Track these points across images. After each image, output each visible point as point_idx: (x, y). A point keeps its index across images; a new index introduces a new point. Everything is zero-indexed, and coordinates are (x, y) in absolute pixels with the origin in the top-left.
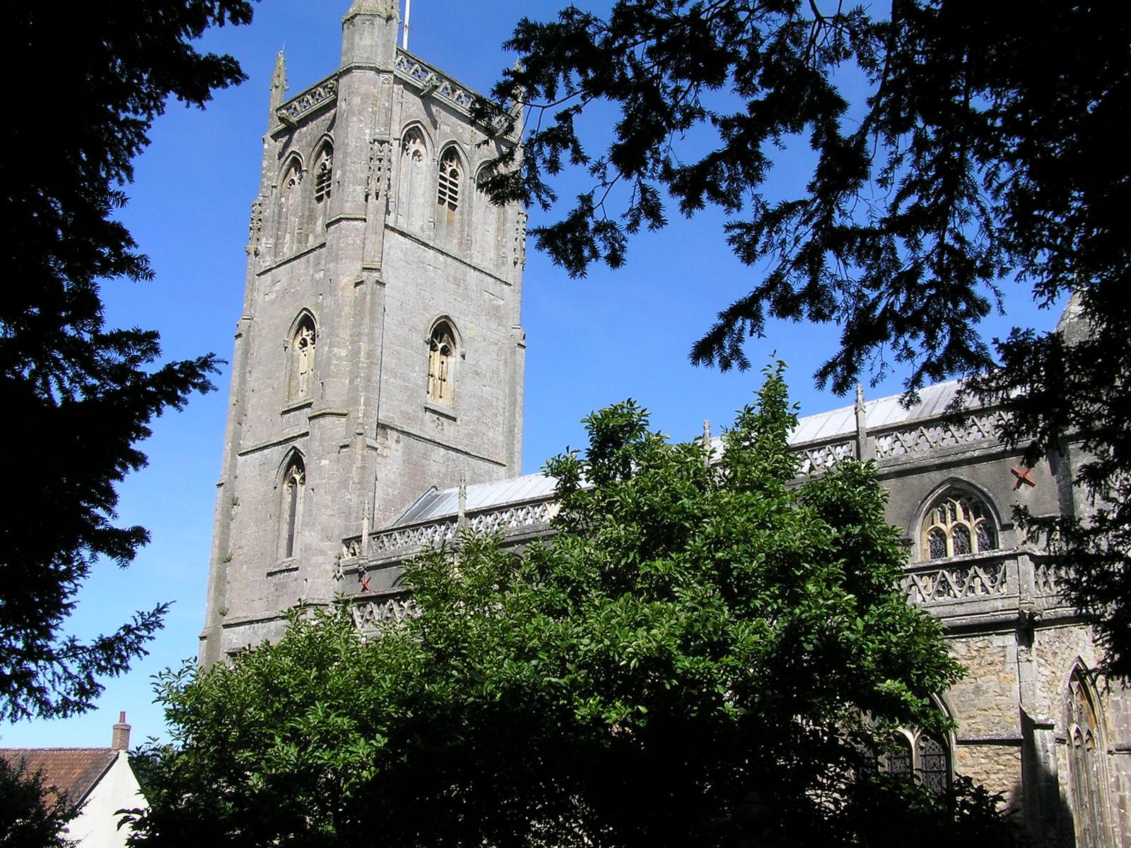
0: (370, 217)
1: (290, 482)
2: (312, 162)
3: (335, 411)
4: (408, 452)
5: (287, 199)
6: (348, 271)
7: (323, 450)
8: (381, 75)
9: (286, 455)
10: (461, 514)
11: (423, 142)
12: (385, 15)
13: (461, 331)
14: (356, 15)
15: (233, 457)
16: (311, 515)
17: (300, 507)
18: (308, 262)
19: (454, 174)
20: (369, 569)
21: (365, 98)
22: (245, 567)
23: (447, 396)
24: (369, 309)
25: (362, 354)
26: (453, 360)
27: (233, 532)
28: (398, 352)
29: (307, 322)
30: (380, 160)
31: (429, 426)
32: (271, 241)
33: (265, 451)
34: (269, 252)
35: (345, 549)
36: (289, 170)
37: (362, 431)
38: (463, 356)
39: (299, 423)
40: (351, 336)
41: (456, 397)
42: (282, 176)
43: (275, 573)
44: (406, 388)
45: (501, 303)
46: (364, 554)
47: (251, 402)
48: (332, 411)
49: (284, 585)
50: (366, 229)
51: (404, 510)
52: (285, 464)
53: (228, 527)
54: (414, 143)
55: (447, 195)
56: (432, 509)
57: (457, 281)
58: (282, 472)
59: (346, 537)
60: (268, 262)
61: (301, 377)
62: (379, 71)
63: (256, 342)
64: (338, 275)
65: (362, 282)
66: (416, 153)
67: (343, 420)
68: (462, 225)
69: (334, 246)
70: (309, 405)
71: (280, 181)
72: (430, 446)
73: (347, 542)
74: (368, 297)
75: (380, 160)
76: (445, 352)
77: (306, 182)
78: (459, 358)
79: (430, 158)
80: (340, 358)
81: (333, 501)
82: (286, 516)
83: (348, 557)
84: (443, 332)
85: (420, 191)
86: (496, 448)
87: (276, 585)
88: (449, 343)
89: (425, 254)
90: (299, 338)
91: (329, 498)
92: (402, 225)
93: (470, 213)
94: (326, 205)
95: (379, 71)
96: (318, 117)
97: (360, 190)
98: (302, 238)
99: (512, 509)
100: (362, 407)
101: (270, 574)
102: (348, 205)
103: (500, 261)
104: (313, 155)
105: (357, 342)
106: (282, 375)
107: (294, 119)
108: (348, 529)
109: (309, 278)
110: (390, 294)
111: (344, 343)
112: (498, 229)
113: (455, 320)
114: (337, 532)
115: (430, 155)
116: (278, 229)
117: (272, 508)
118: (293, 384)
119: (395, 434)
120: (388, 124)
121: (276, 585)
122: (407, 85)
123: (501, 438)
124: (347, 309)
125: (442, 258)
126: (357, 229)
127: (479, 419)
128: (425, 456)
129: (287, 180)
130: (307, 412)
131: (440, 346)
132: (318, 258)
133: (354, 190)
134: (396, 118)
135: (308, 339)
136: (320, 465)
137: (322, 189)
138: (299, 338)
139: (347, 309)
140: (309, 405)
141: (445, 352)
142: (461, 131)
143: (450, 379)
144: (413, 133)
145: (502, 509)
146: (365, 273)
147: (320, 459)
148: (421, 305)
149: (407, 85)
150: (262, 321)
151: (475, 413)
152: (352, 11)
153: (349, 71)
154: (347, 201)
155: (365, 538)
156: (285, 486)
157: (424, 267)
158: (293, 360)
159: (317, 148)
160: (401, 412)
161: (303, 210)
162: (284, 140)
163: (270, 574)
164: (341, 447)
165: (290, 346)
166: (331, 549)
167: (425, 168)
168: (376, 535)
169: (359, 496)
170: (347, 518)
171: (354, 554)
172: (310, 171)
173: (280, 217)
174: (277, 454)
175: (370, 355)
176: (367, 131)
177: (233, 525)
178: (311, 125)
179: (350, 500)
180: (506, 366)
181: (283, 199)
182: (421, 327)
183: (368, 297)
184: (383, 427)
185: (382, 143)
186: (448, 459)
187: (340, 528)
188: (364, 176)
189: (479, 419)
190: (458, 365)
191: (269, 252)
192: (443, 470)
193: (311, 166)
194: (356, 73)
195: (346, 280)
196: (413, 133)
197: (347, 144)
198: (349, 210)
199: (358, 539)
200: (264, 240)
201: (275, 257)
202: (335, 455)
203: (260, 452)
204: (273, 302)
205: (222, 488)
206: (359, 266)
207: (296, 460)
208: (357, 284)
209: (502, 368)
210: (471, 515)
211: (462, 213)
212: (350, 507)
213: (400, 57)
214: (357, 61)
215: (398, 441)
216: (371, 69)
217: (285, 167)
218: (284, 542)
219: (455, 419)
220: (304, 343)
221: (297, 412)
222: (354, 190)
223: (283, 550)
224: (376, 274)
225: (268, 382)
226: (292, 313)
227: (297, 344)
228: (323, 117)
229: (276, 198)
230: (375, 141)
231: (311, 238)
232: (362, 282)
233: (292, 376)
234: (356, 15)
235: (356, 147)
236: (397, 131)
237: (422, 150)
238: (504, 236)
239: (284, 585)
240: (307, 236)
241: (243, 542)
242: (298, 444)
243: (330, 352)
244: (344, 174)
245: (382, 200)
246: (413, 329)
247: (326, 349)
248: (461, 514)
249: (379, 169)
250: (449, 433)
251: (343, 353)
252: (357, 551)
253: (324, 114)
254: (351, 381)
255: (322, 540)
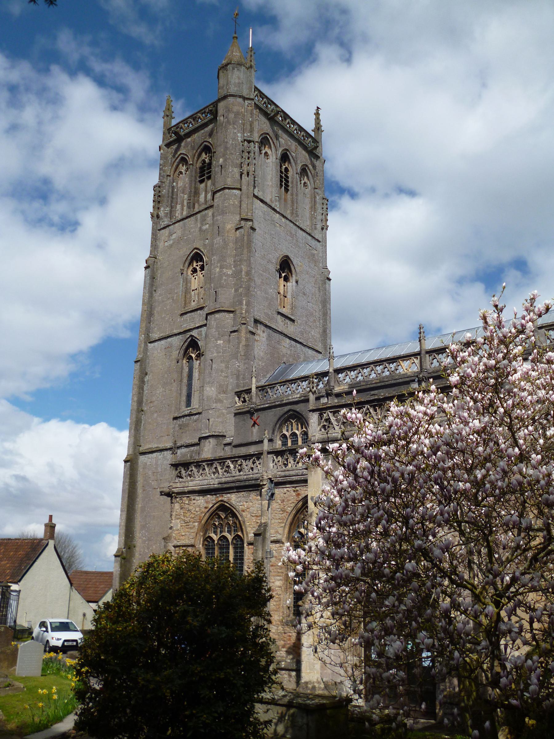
0: (244, 188)
1: (188, 359)
2: (196, 159)
3: (226, 309)
4: (269, 337)
5: (177, 184)
6: (230, 223)
7: (219, 334)
8: (246, 101)
9: (185, 341)
10: (331, 371)
11: (270, 147)
12: (248, 65)
13: (296, 266)
14: (228, 64)
15: (145, 343)
16: (211, 377)
17: (196, 374)
18: (196, 220)
19: (287, 170)
20: (258, 410)
21: (237, 114)
22: (156, 415)
23: (288, 307)
24: (245, 245)
25: (243, 273)
26: (291, 284)
27: (146, 392)
28: (262, 275)
29: (197, 257)
30: (249, 153)
31: (280, 324)
32: (168, 209)
33: (169, 340)
34: (166, 216)
35: (237, 399)
36: (177, 166)
37: (244, 322)
38: (297, 282)
39: (198, 319)
40: (234, 261)
41: (293, 307)
42: (173, 169)
43: (180, 417)
44: (267, 298)
45: (316, 252)
46: (254, 400)
47: (156, 309)
48: (223, 309)
49: (187, 425)
50: (241, 195)
51: (268, 376)
52: (184, 347)
53: (142, 389)
54: (265, 148)
55: (284, 181)
56: (293, 371)
57: (292, 235)
58: (182, 352)
59: (237, 390)
60: (166, 222)
61: (193, 293)
62: (245, 99)
63: (159, 272)
64: (224, 223)
65: (241, 227)
66: (266, 153)
67: (232, 315)
68: (293, 202)
69: (221, 206)
70: (201, 308)
71: (172, 173)
72: (281, 337)
73: (239, 394)
74: (245, 238)
75: (249, 153)
76: (286, 279)
77: (192, 172)
78: (294, 283)
79: (274, 157)
80: (228, 275)
81: (227, 367)
82: (185, 381)
83: (239, 404)
84: (285, 266)
85: (269, 177)
86: (316, 341)
87: (179, 425)
88: (288, 274)
89: (274, 216)
90: (191, 268)
91: (223, 365)
92: (260, 195)
93: (297, 195)
94: (206, 186)
95: (245, 99)
96: (198, 131)
97: (236, 171)
98: (191, 205)
99: (372, 365)
100: (244, 307)
101: (175, 418)
102: (229, 179)
103: (313, 227)
104: (197, 155)
105: (240, 265)
106: (180, 290)
107: (182, 133)
108: (238, 386)
109: (197, 229)
110: (257, 237)
111: (230, 266)
112: (311, 208)
113: (292, 259)
114: (230, 387)
115: (274, 155)
116: (172, 202)
117: (175, 376)
118: (188, 296)
119: (263, 328)
120: (251, 131)
121: (179, 425)
122: (260, 109)
123: (318, 336)
124: (231, 245)
125: (283, 220)
126: (235, 195)
127: (306, 322)
128: (279, 342)
129: (177, 172)
130: (203, 313)
131: (283, 275)
132: (205, 216)
133: (233, 171)
134: (256, 130)
135: (198, 268)
136: (214, 344)
137: (204, 175)
138: (191, 268)
139: (231, 245)
140: (201, 308)
141: (286, 279)
142: (290, 144)
143: (289, 296)
144: (264, 141)
145: (363, 366)
146: (243, 223)
147: (216, 340)
148: (273, 248)
149: (260, 109)
150: (163, 259)
151: (304, 319)
152: (224, 62)
153: (225, 97)
154: (228, 177)
155: (254, 389)
156: (184, 361)
157: (274, 224)
158: (187, 282)
159: (199, 150)
160: (265, 313)
161: (190, 188)
162: (174, 147)
163: (175, 418)
164: (231, 332)
165: (185, 272)
166: (226, 399)
167: (271, 163)
168: (261, 388)
169: (245, 364)
170: (238, 378)
171: (243, 402)
172: (195, 165)
173: (173, 195)
174: (177, 342)
175: (248, 273)
176: (239, 135)
177: (145, 388)
178: (196, 136)
179: (239, 366)
180: (320, 291)
181: (175, 184)
182: (274, 261)
183: (245, 238)
184: (256, 321)
185: (249, 142)
186: (291, 346)
187: (232, 384)
188: (239, 162)
189: (306, 322)
190: (294, 287)
191: (166, 216)
192: (289, 352)
193: (195, 161)
194: (230, 99)
195: (230, 227)
196: (264, 141)
197: (227, 142)
198: (229, 182)
199: (249, 391)
200: (162, 209)
201: (171, 219)
202: (226, 337)
203: (165, 341)
204: (171, 246)
205: (139, 364)
206: (238, 218)
207: (193, 344)
208: (237, 229)
209: (317, 292)
210: (338, 371)
211: (292, 195)
212: (239, 371)
213: (256, 92)
214: (233, 90)
215: (264, 332)
216: (240, 97)
217: (176, 164)
218: (184, 398)
219: (293, 321)
220: (195, 271)
221: (193, 314)
222: (233, 171)
223: (183, 404)
224: (250, 223)
225: (169, 296)
226: (185, 251)
227: (190, 272)
228: (202, 131)
229: (170, 183)
230: (245, 140)
231: (196, 206)
232: (241, 227)
233: (187, 291)
234: (228, 64)
235: (232, 144)
236: (256, 137)
237: (269, 152)
238: (315, 211)
239: (187, 425)
240: (194, 204)
241: (154, 399)
242: (194, 333)
243: (221, 272)
244: (225, 160)
245: (251, 177)
246: (269, 261)
247: (218, 270)
248: (331, 371)
249: (248, 158)
250: (290, 329)
251: (230, 272)
252: (247, 399)
253: (203, 129)
254: (236, 290)
255: (219, 393)
